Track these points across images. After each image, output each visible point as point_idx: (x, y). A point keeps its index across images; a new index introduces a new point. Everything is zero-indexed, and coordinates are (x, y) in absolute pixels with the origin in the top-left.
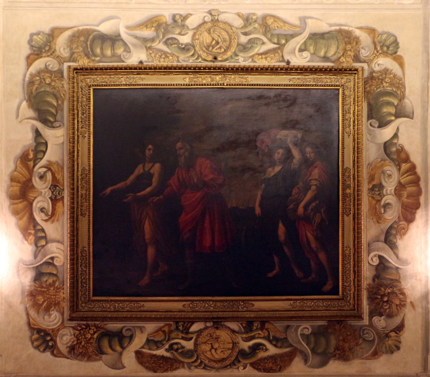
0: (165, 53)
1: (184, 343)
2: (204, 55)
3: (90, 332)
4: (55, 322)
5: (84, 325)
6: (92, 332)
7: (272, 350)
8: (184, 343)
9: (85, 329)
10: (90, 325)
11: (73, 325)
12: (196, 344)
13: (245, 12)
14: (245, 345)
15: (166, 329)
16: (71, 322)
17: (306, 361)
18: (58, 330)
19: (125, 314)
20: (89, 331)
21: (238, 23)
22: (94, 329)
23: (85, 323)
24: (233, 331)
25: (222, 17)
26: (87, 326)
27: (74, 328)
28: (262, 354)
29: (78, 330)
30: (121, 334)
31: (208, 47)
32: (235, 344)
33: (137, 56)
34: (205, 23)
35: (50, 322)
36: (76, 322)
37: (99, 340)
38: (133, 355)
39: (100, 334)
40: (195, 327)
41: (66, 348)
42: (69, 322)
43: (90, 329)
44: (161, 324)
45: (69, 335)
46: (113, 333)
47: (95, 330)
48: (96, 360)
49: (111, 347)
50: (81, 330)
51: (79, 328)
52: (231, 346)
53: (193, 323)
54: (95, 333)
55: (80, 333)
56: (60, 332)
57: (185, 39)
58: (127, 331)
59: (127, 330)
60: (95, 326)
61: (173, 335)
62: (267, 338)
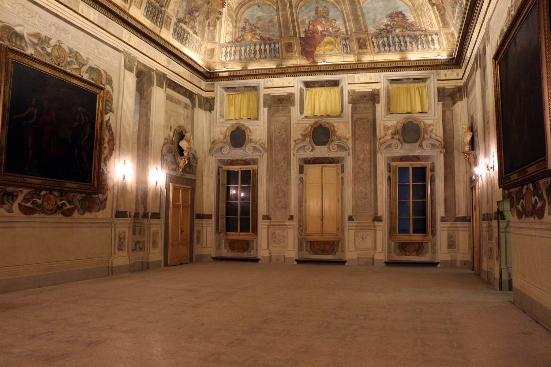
0: (41, 54)
1: (38, 200)
2: (55, 61)
7: (69, 206)
8: (38, 200)
12: (42, 202)
13: (70, 47)
14: (60, 203)
15: (32, 193)
17: (79, 212)
19: (17, 184)
21: (68, 51)
24: (56, 196)
25: (63, 45)
28: (66, 208)
31: (57, 57)
32: (56, 202)
33: (30, 51)
34: (56, 45)
40: (43, 193)
44: (30, 190)
52: (54, 203)
53: (42, 191)
57: (49, 50)
61: (34, 196)
62: (66, 200)
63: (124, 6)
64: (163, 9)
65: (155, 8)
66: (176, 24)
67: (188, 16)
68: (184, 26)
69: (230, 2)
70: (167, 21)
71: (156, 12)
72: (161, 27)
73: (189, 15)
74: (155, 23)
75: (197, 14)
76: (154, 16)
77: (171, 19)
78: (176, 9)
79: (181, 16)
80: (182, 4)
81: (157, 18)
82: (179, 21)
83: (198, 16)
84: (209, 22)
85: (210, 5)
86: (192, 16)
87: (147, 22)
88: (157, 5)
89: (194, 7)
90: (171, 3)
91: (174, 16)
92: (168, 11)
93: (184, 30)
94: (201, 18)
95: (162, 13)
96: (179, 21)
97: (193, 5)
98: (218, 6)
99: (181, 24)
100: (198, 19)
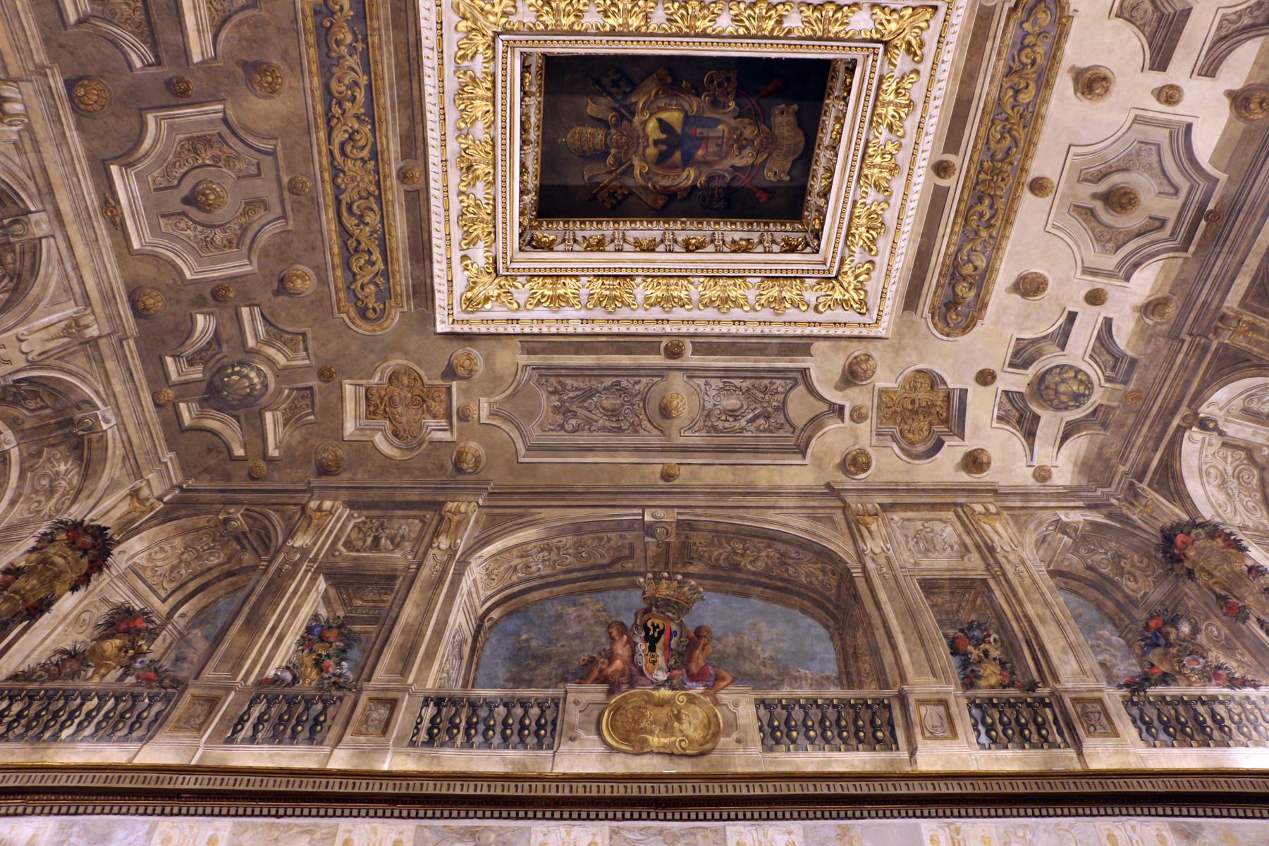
63: (892, 762)
64: (1043, 691)
65: (1012, 706)
66: (1128, 703)
67: (1154, 656)
68: (1171, 691)
69: (1237, 521)
70: (1085, 715)
71: (1024, 709)
72: (1078, 744)
73: (1158, 651)
74: (1044, 742)
75: (1185, 629)
76: (1023, 727)
77: (1100, 701)
78: (1091, 662)
79: (1128, 668)
80: (1099, 638)
81: (1039, 727)
82: (1135, 686)
83: (1195, 630)
84: (1259, 620)
85: (1202, 578)
86: (1169, 644)
87: (1010, 760)
88: (1012, 692)
89: (1152, 617)
90: (1055, 661)
91: (1104, 684)
92: (1069, 685)
93: (1180, 700)
94: (1215, 627)
95: (1050, 705)
96: (1135, 686)
97: (1141, 615)
98: (1226, 559)
99: (1153, 691)
100: (1202, 639)
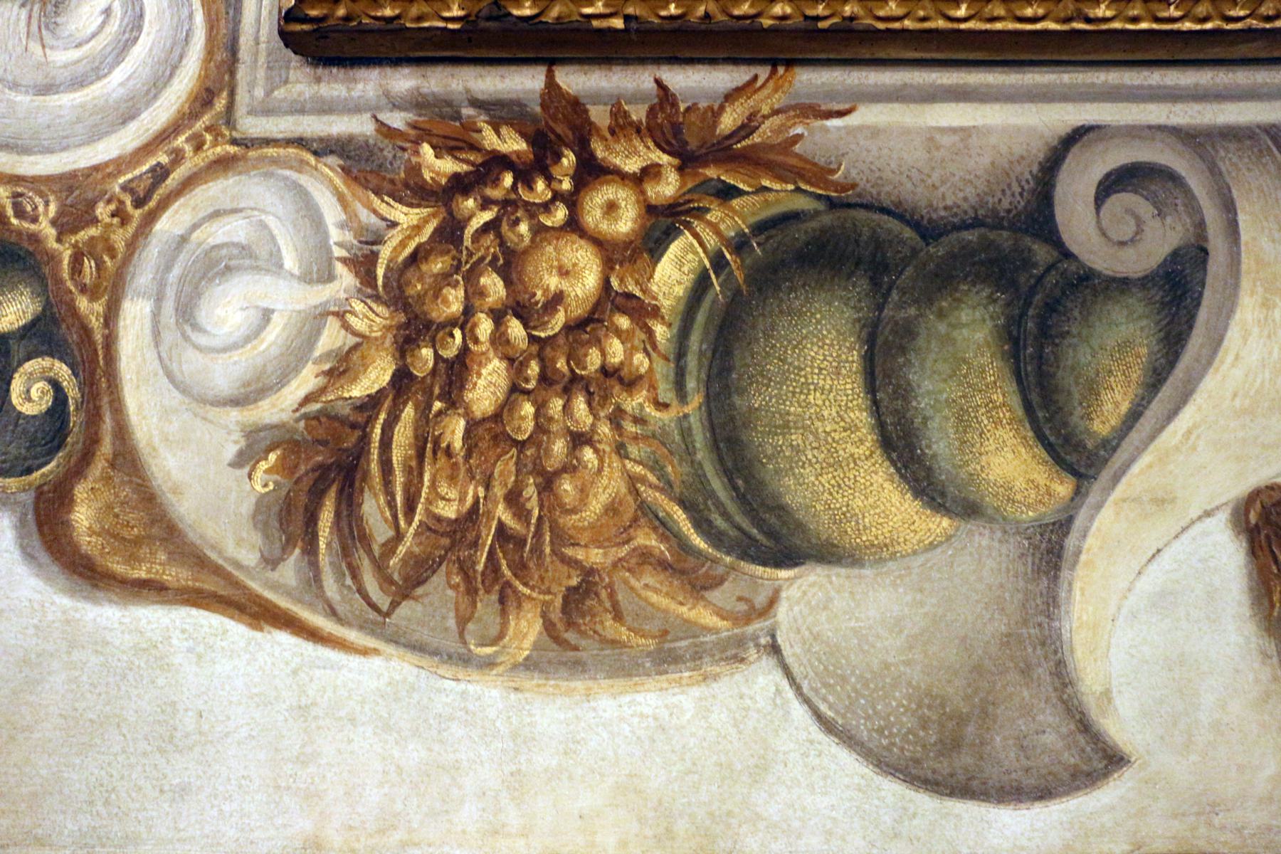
3: (593, 215)
4: (115, 83)
5: (503, 112)
6: (625, 224)
9: (524, 176)
10: (599, 115)
11: (359, 126)
16: (335, 85)
18: (151, 195)
20: (572, 201)
22: (650, 172)
23: (524, 82)
26: (559, 134)
27: (361, 165)
29: (416, 191)
30: (1042, 253)
35: (47, 89)
36: (404, 81)
37: (728, 328)
38: (1224, 556)
39: (740, 245)
41: (246, 459)
42: (302, 82)
43: (592, 171)
45: (290, 262)
46: (929, 230)
47: (668, 187)
48: (671, 654)
49: (901, 445)
50: (459, 185)
51: (438, 166)
54: (662, 224)
55: (450, 232)
56: (169, 224)
58: (1120, 201)
59: (1117, 182)
60: (667, 125)
